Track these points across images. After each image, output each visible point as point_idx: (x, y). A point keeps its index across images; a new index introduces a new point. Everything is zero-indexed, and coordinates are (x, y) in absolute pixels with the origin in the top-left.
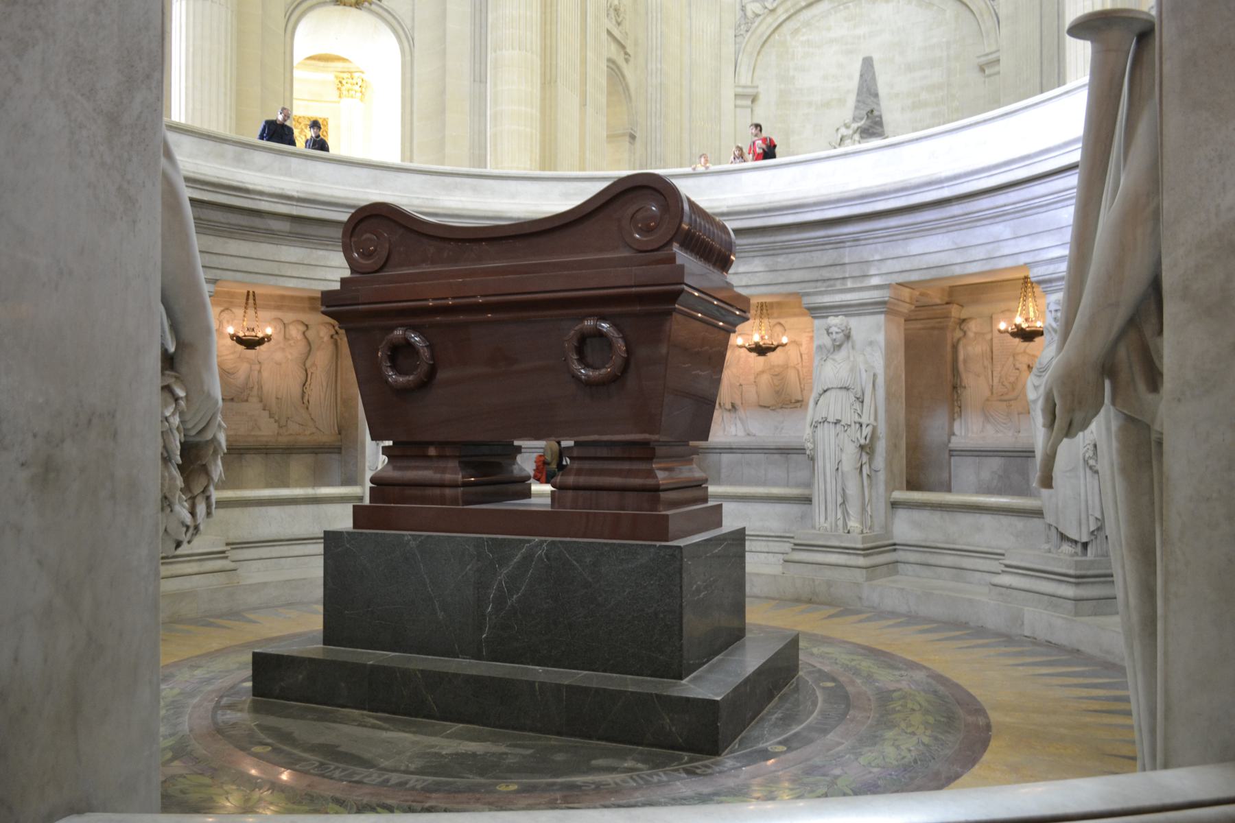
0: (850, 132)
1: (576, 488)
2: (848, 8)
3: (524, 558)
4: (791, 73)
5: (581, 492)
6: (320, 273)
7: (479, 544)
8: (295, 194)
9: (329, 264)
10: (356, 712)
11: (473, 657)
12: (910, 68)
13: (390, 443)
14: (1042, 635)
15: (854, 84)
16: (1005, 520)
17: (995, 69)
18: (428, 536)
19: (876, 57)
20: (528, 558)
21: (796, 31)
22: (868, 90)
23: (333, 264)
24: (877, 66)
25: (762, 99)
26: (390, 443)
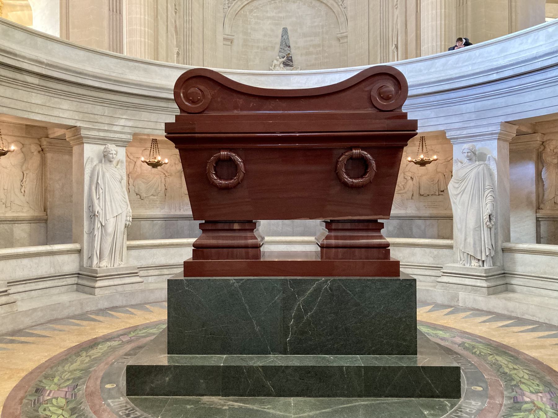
0: (279, 63)
1: (337, 247)
2: (276, 3)
3: (315, 290)
4: (249, 31)
5: (340, 250)
6: (56, 113)
7: (284, 282)
8: (46, 61)
9: (61, 107)
10: (215, 399)
11: (281, 353)
12: (305, 35)
13: (204, 221)
14: (470, 305)
15: (279, 40)
16: (428, 250)
17: (345, 40)
18: (248, 280)
19: (289, 28)
20: (318, 290)
21: (251, 11)
22: (285, 44)
23: (64, 107)
24: (289, 33)
25: (235, 42)
26: (204, 221)
